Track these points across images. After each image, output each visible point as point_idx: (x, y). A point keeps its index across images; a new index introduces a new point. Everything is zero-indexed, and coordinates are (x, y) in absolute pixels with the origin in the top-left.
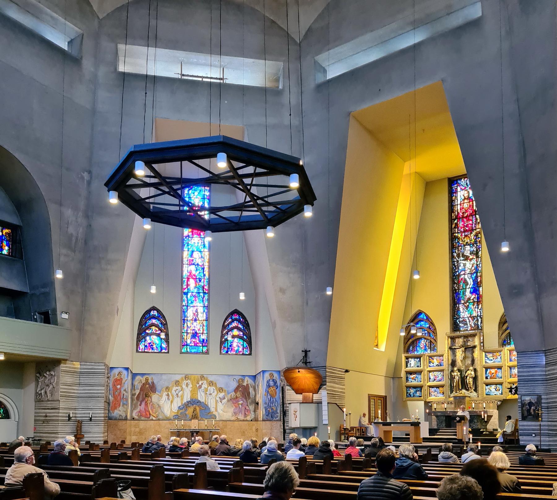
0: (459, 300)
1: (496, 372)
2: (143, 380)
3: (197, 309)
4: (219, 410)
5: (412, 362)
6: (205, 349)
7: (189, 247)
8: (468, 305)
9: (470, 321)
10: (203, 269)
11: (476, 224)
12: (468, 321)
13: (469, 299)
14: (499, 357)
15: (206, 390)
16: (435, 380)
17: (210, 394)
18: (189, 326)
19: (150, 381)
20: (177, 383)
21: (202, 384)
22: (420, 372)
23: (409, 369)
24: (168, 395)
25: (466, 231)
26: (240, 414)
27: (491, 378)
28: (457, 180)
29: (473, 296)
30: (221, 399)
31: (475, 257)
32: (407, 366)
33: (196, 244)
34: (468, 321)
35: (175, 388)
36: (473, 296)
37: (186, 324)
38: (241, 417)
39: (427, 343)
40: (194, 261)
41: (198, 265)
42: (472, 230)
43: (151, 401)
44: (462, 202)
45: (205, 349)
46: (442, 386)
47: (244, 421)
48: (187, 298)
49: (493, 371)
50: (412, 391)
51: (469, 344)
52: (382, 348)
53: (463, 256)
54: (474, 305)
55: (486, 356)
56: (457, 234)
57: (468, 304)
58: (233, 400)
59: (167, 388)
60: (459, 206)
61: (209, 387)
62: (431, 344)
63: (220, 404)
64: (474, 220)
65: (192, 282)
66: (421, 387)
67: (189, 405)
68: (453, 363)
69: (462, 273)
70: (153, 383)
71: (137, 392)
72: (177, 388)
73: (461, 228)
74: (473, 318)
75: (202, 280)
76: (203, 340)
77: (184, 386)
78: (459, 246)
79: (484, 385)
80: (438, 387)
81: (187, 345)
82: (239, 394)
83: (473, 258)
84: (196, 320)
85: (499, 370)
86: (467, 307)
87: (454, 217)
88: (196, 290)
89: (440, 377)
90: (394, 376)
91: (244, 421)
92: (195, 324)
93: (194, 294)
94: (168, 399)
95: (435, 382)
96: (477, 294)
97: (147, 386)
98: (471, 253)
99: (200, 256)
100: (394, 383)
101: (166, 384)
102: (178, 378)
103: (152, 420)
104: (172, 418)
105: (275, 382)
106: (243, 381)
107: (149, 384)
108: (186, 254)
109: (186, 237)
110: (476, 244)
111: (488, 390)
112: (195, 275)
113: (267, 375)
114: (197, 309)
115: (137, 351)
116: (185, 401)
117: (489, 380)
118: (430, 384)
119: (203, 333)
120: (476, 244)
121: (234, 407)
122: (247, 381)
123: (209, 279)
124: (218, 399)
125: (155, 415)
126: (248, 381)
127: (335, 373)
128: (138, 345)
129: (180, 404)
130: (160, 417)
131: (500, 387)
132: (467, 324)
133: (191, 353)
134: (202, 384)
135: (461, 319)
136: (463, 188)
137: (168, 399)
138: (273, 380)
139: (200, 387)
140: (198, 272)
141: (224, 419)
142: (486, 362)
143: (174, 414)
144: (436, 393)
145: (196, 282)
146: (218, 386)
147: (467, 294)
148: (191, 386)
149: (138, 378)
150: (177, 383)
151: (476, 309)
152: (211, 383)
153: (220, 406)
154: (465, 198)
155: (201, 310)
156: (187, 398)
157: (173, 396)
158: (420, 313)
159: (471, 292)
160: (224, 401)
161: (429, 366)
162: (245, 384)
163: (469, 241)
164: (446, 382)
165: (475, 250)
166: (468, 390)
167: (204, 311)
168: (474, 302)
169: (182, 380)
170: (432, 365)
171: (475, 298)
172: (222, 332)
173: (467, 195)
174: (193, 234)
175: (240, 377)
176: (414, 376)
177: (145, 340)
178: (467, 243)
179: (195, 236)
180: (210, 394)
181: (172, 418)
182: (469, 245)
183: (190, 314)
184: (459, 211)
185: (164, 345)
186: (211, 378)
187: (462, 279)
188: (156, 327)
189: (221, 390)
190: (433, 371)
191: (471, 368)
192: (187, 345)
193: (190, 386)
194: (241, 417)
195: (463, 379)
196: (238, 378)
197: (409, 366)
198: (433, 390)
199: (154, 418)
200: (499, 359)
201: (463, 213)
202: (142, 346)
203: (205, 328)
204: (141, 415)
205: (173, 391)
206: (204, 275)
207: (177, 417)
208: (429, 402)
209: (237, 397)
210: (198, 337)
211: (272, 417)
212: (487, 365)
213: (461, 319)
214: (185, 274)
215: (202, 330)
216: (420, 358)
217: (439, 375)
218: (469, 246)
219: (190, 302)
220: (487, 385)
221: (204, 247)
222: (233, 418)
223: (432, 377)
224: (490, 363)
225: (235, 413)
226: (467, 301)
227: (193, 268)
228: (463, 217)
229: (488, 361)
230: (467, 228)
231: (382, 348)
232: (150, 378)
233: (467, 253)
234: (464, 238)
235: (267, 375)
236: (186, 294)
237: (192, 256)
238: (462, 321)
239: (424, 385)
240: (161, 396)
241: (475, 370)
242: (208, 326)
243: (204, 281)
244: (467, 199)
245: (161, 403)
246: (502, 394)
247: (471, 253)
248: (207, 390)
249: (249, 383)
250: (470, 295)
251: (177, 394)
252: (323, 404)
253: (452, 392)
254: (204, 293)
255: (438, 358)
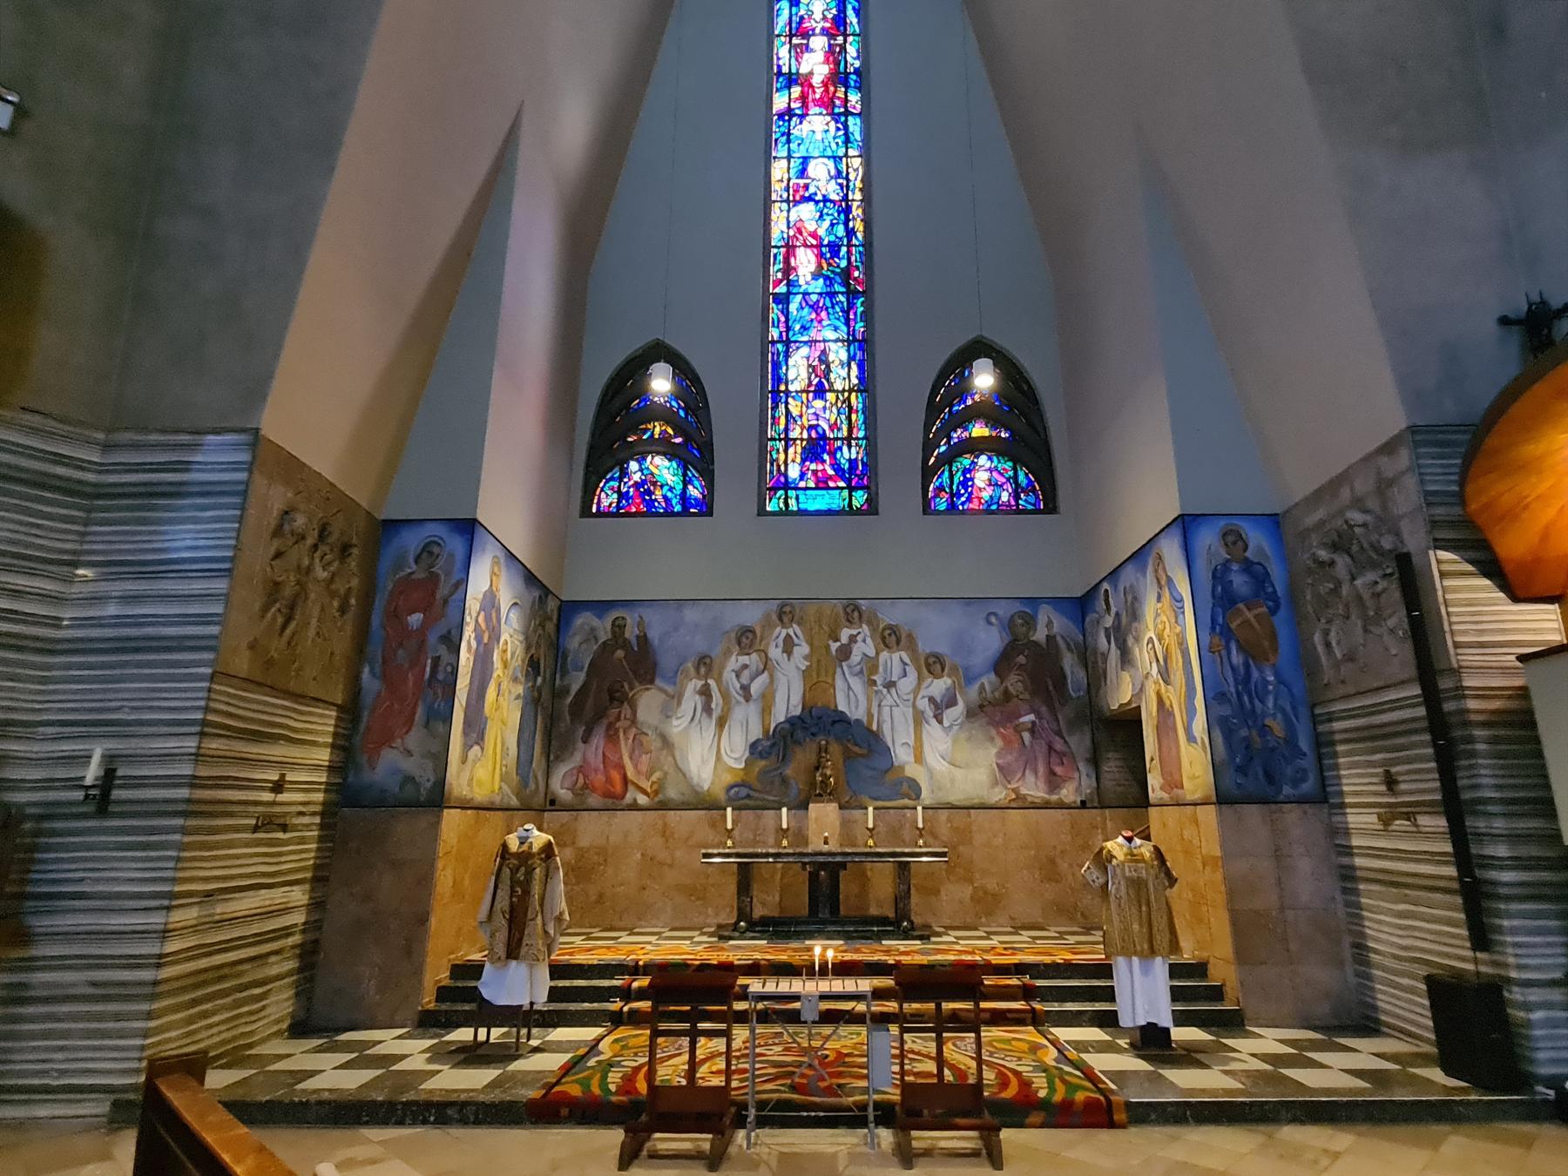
2: (603, 627)
3: (824, 352)
4: (932, 758)
6: (860, 498)
7: (793, 146)
10: (847, 211)
15: (871, 665)
17: (890, 685)
18: (795, 412)
19: (631, 633)
20: (746, 639)
21: (853, 639)
24: (705, 692)
26: (1030, 777)
30: (939, 707)
33: (819, 136)
35: (735, 662)
37: (782, 407)
38: (1034, 788)
40: (812, 190)
41: (826, 200)
43: (634, 721)
45: (860, 498)
47: (1046, 805)
48: (786, 313)
58: (990, 712)
59: (705, 664)
61: (884, 655)
63: (933, 731)
65: (805, 262)
67: (799, 734)
70: (643, 640)
71: (577, 681)
72: (744, 659)
75: (844, 250)
76: (853, 463)
77: (775, 653)
81: (786, 486)
82: (1014, 683)
84: (820, 392)
88: (819, 286)
91: (1046, 805)
92: (819, 404)
93: (814, 298)
94: (707, 709)
97: (620, 653)
99: (833, 172)
101: (700, 644)
102: (751, 615)
103: (634, 807)
104: (722, 796)
105: (1258, 576)
106: (1030, 621)
107: (625, 644)
108: (779, 170)
109: (781, 116)
112: (814, 235)
113: (1207, 538)
114: (824, 352)
115: (585, 512)
116: (779, 715)
119: (849, 439)
121: (999, 742)
122: (1049, 624)
123: (868, 244)
124: (923, 704)
125: (646, 785)
126: (1049, 625)
128: (589, 491)
129: (756, 733)
130: (672, 793)
133: (802, 513)
134: (853, 639)
137: (707, 709)
138: (1248, 566)
139: (845, 653)
140: (826, 224)
141: (954, 798)
143: (728, 779)
145: (820, 256)
146: (924, 647)
148: (805, 649)
149: (583, 620)
150: (746, 639)
152: (891, 637)
153: (937, 740)
155: (838, 353)
156: (788, 701)
157: (726, 696)
160: (952, 715)
162: (1040, 635)
167: (851, 358)
169: (768, 625)
172: (927, 429)
174: (805, 105)
175: (1017, 607)
177: (624, 473)
179: (814, 110)
180: (890, 685)
181: (722, 796)
183: (798, 370)
185: (694, 492)
186: (891, 615)
188: (668, 423)
189: (933, 665)
192: (786, 486)
193: (802, 649)
194: (1034, 788)
196: (1005, 610)
199: (642, 800)
202: (608, 499)
203: (858, 418)
204: (585, 786)
205: (729, 675)
206: (850, 233)
207: (748, 795)
209: (1007, 695)
210: (832, 454)
211: (1270, 778)
214: (778, 230)
215: (845, 427)
219: (797, 327)
221: (847, 141)
222: (999, 795)
225: (1005, 772)
227: (806, 213)
232: (631, 619)
235: (1207, 538)
236: (784, 300)
237: (803, 173)
240: (678, 698)
242: (870, 412)
243: (849, 252)
245: (677, 726)
248: (874, 669)
249: (1056, 629)
251: (745, 689)
254: (852, 295)
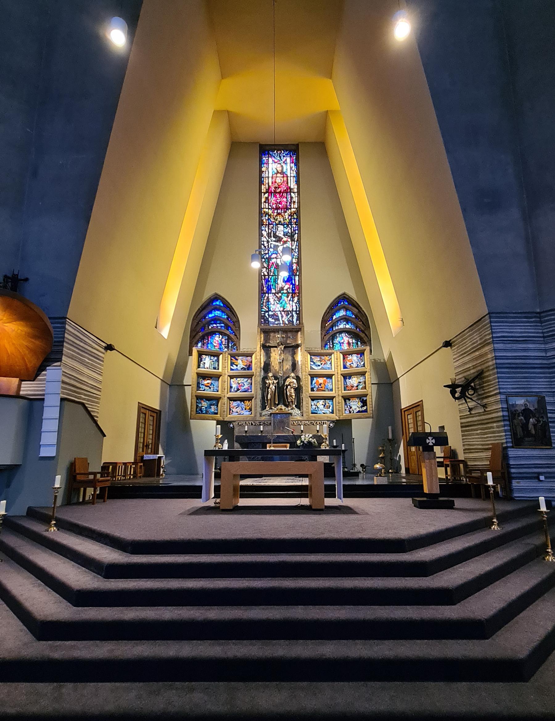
0: (269, 289)
1: (325, 381)
5: (207, 361)
8: (281, 297)
9: (282, 317)
11: (290, 203)
12: (280, 315)
13: (282, 289)
14: (329, 362)
16: (238, 390)
22: (217, 377)
23: (201, 370)
25: (277, 208)
27: (318, 390)
28: (268, 151)
29: (287, 286)
31: (289, 240)
32: (199, 366)
34: (280, 315)
36: (287, 286)
39: (223, 340)
42: (286, 209)
44: (275, 175)
46: (250, 399)
49: (321, 380)
50: (205, 404)
51: (288, 342)
52: (165, 332)
53: (275, 236)
54: (288, 297)
55: (312, 361)
56: (267, 210)
57: (280, 294)
60: (270, 179)
62: (228, 342)
64: (289, 199)
66: (218, 399)
68: (267, 367)
69: (274, 256)
73: (273, 204)
74: (287, 313)
78: (269, 224)
79: (310, 400)
80: (242, 400)
83: (287, 241)
85: (329, 380)
86: (280, 299)
87: (264, 190)
89: (246, 386)
90: (174, 383)
95: (238, 393)
96: (292, 283)
98: (285, 234)
100: (170, 393)
110: (291, 225)
111: (314, 407)
117: (316, 393)
118: (232, 394)
120: (291, 225)
127: (85, 343)
131: (331, 403)
132: (278, 320)
135: (270, 313)
136: (276, 161)
142: (311, 368)
144: (239, 410)
147: (279, 282)
151: (291, 302)
154: (278, 172)
158: (216, 297)
159: (284, 281)
161: (231, 369)
163: (282, 220)
164: (256, 391)
165: (290, 232)
166: (287, 406)
168: (288, 293)
170: (234, 367)
171: (289, 288)
173: (281, 169)
176: (208, 381)
178: (280, 222)
182: (283, 225)
184: (270, 184)
187: (273, 263)
190: (237, 377)
191: (293, 375)
195: (281, 390)
197: (202, 365)
198: (235, 404)
200: (328, 366)
201: (275, 188)
208: (230, 422)
212: (313, 372)
213: (270, 313)
216: (218, 356)
217: (245, 383)
218: (282, 226)
220: (313, 400)
223: (234, 386)
224: (317, 370)
226: (279, 292)
228: (275, 192)
229: (314, 367)
230: (280, 205)
231: (165, 332)
233: (280, 234)
234: (277, 216)
238: (272, 315)
239: (222, 395)
241: (298, 379)
244: (280, 173)
246: (332, 412)
247: (285, 234)
250: (284, 284)
252: (46, 403)
253: (263, 408)
255: (244, 358)
